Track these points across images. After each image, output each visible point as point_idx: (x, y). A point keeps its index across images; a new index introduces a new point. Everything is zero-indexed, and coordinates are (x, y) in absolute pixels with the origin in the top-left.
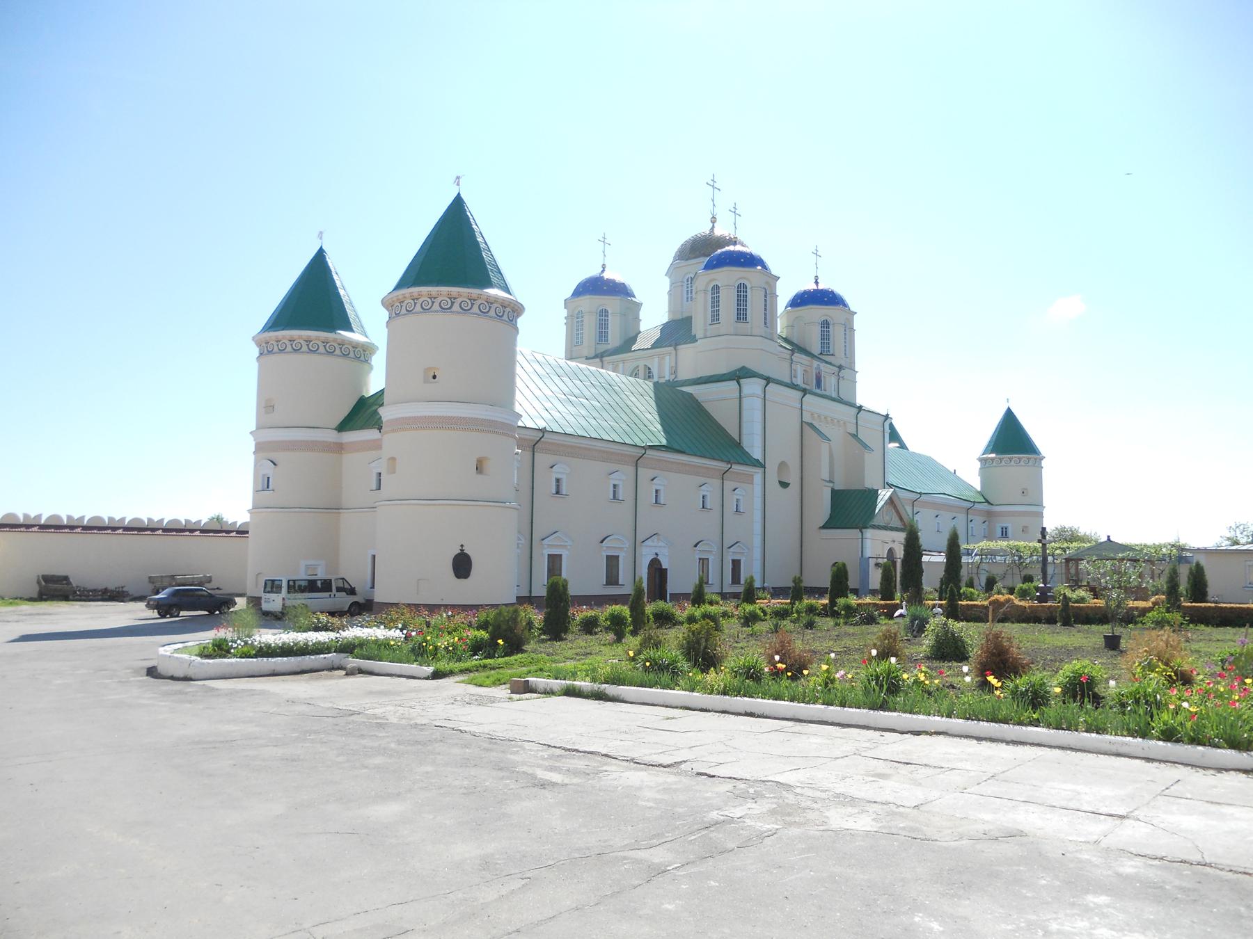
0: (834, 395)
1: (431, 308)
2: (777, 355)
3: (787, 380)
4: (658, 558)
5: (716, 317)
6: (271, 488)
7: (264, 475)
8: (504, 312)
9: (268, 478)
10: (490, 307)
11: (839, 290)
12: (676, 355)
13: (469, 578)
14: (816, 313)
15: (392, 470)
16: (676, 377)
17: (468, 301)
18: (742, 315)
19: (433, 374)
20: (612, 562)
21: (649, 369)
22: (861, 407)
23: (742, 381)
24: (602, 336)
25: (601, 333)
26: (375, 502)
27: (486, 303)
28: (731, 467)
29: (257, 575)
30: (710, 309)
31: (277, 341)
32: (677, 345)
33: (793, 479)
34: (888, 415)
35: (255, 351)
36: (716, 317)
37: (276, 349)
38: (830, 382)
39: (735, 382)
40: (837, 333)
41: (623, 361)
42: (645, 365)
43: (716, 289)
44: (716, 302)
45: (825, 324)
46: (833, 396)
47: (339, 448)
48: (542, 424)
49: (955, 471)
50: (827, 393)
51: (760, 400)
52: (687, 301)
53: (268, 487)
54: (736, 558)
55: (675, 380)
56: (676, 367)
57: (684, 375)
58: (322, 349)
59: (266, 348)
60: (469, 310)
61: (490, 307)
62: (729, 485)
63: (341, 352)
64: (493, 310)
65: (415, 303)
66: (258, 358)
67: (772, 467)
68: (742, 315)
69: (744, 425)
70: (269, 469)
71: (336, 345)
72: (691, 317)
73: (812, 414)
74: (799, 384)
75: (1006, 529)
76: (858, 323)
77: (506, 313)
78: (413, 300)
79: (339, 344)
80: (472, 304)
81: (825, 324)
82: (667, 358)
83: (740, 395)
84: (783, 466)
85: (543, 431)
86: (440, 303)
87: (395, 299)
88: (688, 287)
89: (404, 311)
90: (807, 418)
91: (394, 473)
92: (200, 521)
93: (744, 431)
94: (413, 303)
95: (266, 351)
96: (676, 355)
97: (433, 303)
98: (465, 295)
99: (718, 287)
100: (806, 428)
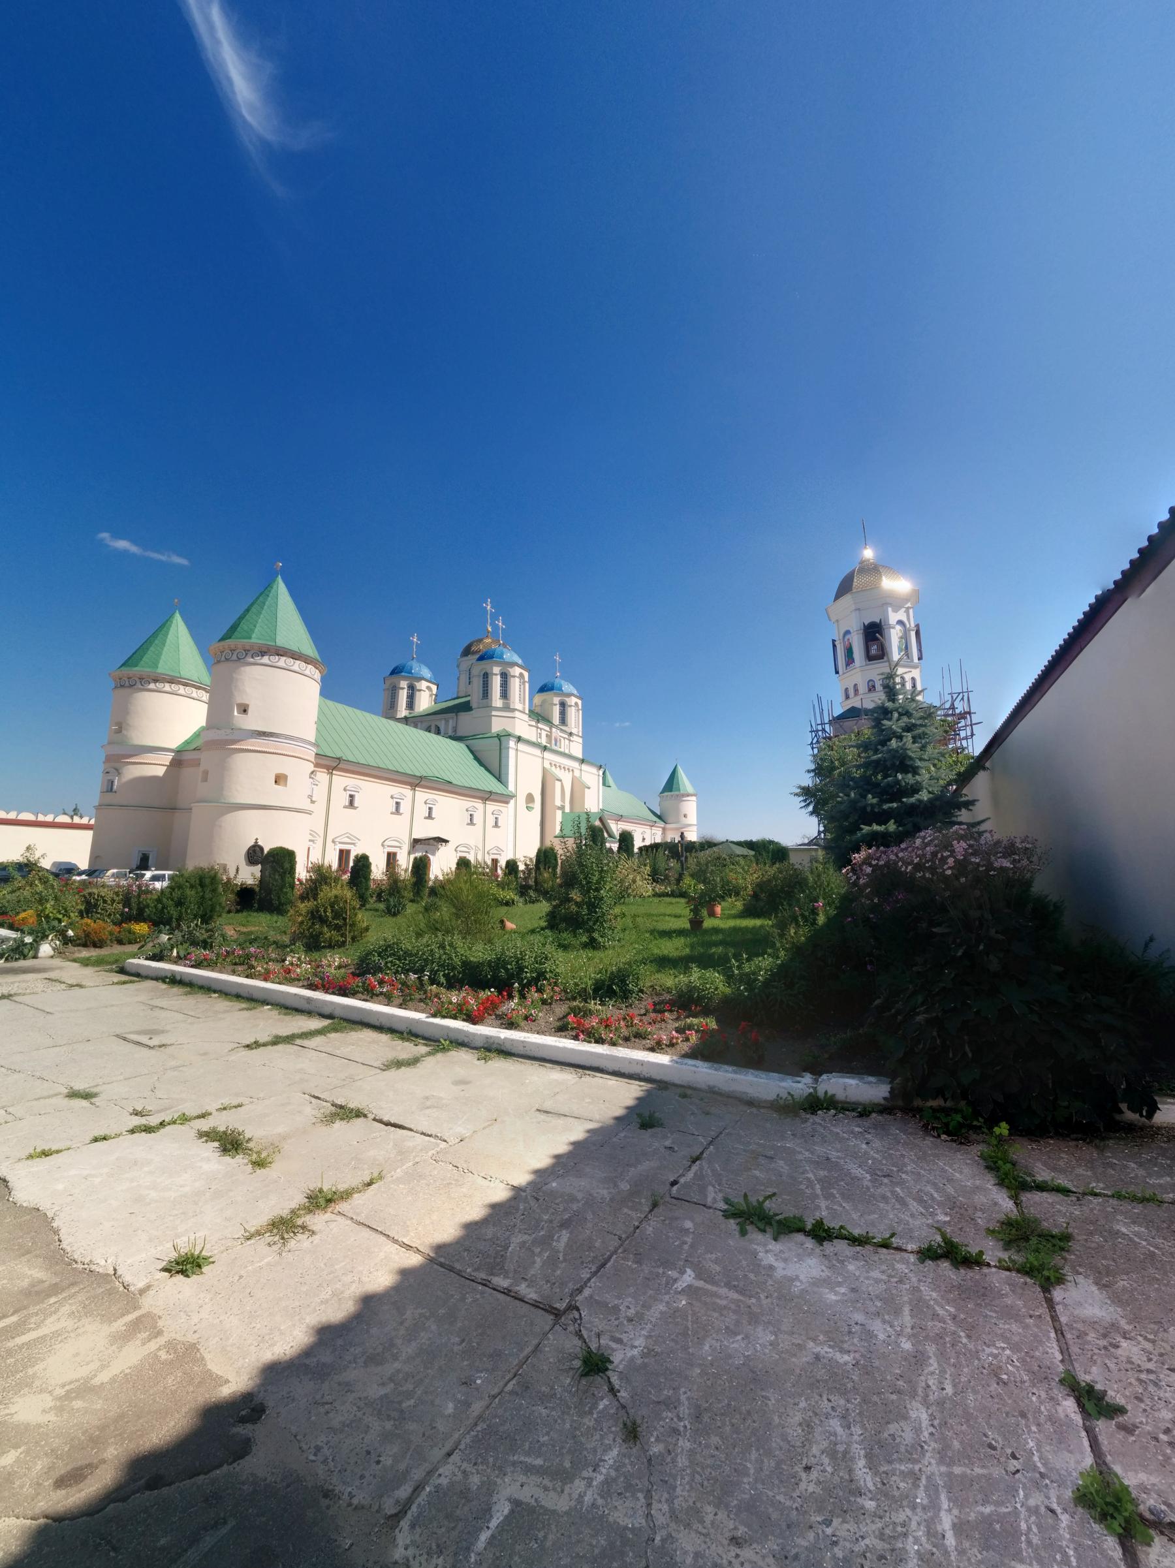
0: (567, 752)
3: (534, 739)
15: (205, 779)
18: (505, 694)
23: (502, 738)
24: (411, 705)
36: (486, 693)
41: (421, 722)
48: (338, 756)
50: (562, 750)
68: (505, 694)
69: (503, 767)
82: (451, 721)
85: (339, 759)
89: (223, 659)
90: (547, 765)
93: (503, 772)
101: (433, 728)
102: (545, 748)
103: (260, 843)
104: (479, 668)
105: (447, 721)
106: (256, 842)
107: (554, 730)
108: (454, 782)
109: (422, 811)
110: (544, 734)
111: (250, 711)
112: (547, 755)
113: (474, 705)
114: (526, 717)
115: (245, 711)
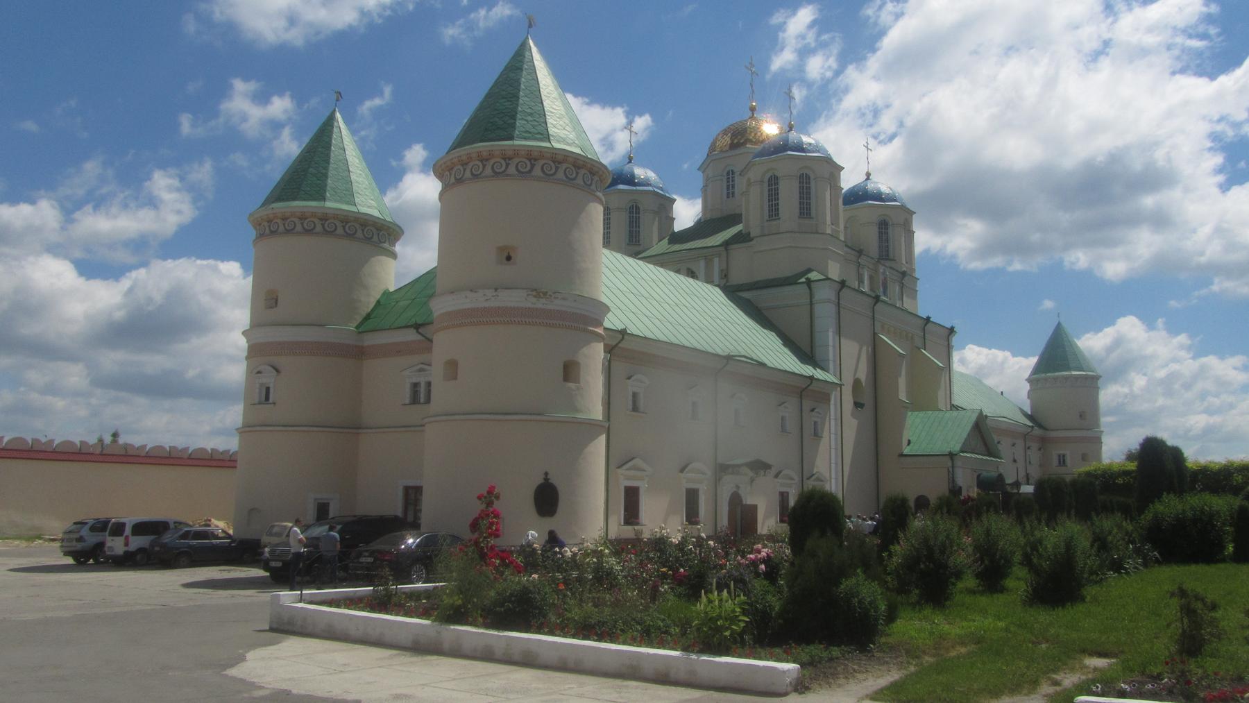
1: (505, 171)
4: (740, 492)
6: (271, 400)
7: (262, 385)
8: (592, 180)
9: (268, 389)
10: (577, 173)
13: (557, 514)
16: (727, 282)
17: (552, 164)
18: (805, 210)
19: (506, 254)
20: (692, 498)
23: (813, 285)
26: (423, 419)
29: (252, 509)
31: (283, 219)
35: (253, 233)
37: (281, 228)
39: (805, 286)
43: (774, 181)
45: (883, 226)
46: (898, 305)
47: (358, 353)
49: (1002, 393)
51: (834, 306)
52: (728, 197)
53: (267, 398)
54: (784, 489)
55: (728, 284)
58: (340, 231)
59: (267, 229)
60: (552, 175)
61: (577, 173)
62: (807, 405)
63: (364, 235)
64: (580, 176)
65: (484, 166)
66: (254, 241)
70: (269, 378)
71: (358, 226)
75: (1064, 456)
77: (594, 182)
78: (481, 161)
79: (362, 225)
80: (557, 168)
82: (716, 260)
83: (811, 302)
84: (857, 383)
86: (517, 164)
87: (455, 160)
88: (728, 182)
89: (468, 174)
91: (455, 378)
92: (188, 448)
94: (481, 166)
95: (267, 231)
97: (507, 165)
99: (776, 178)
103: (554, 480)
106: (546, 480)
108: (770, 364)
113: (754, 232)
115: (509, 258)
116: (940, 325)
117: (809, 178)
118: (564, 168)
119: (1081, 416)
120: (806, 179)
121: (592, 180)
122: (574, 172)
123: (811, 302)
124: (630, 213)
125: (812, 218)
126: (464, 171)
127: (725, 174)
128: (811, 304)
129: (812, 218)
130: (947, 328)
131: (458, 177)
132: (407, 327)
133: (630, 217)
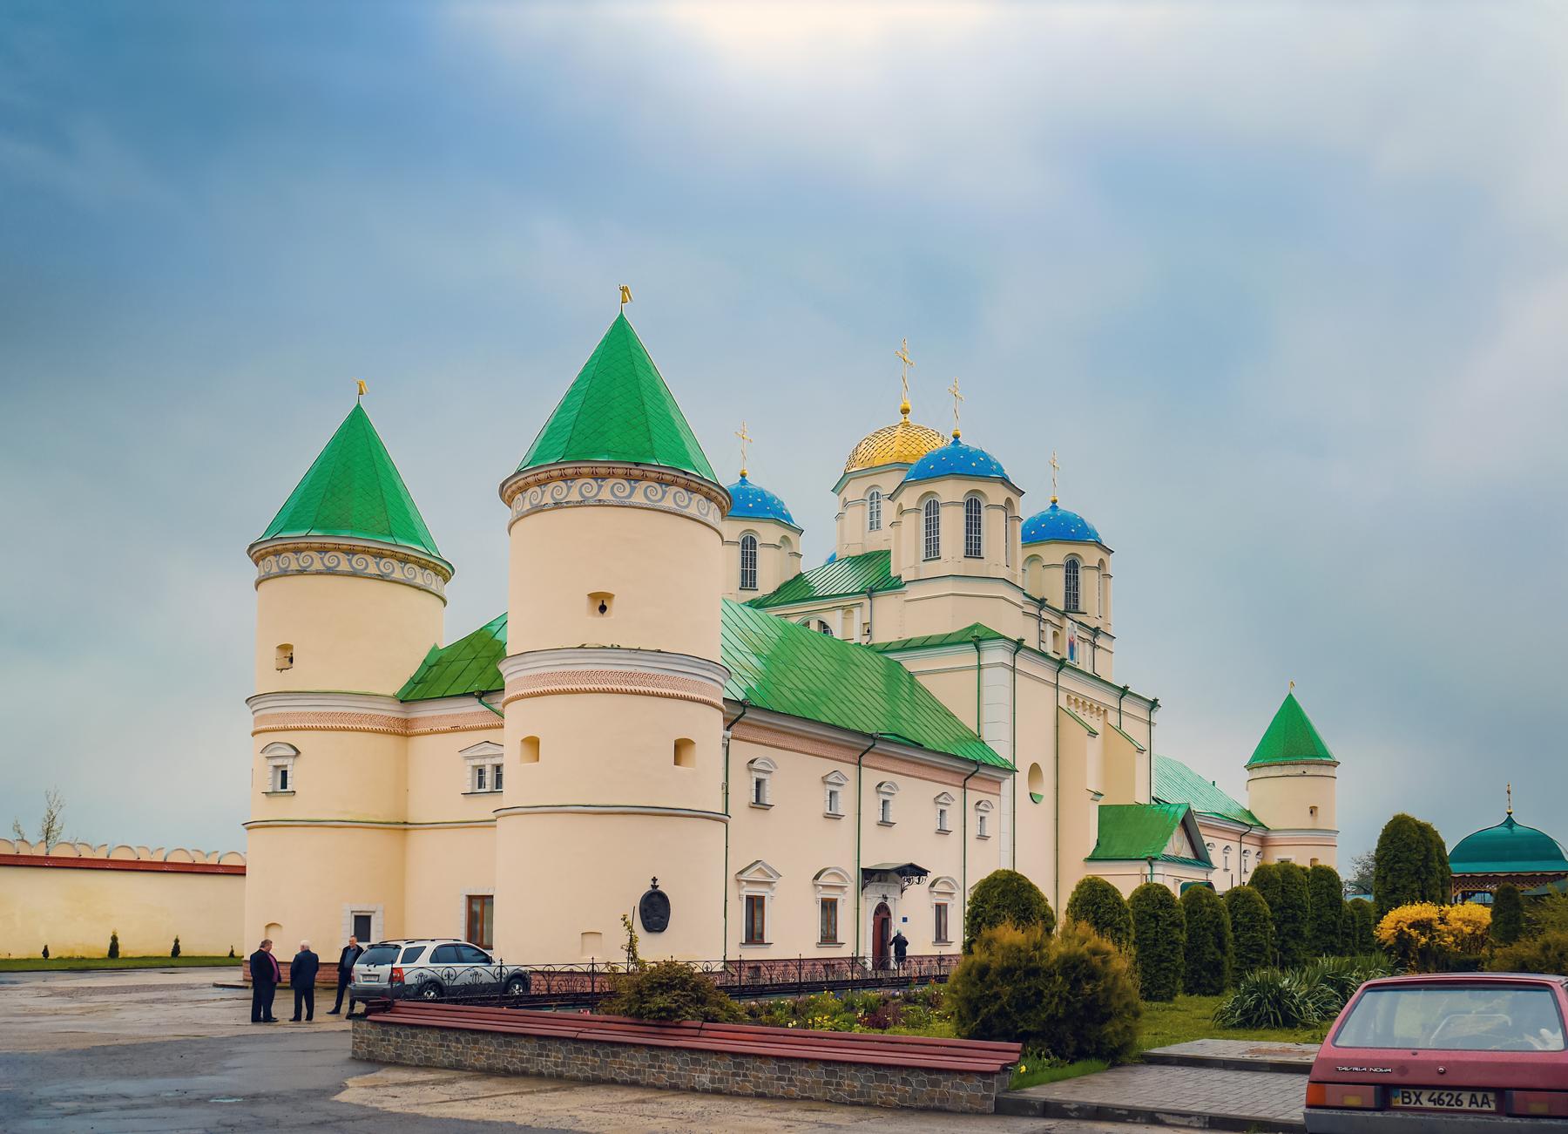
0: (1089, 671)
1: (596, 495)
2: (1022, 608)
5: (932, 550)
6: (289, 788)
8: (709, 507)
10: (690, 499)
11: (1094, 521)
12: (871, 606)
14: (1056, 554)
18: (973, 550)
21: (825, 626)
22: (1124, 691)
23: (983, 645)
25: (744, 574)
27: (684, 491)
28: (975, 772)
30: (923, 538)
32: (871, 593)
33: (1046, 789)
34: (1156, 700)
36: (932, 550)
38: (1083, 651)
39: (972, 646)
40: (1087, 580)
42: (821, 622)
43: (932, 510)
44: (932, 527)
45: (1072, 567)
51: (1008, 671)
52: (871, 529)
53: (284, 785)
56: (870, 623)
57: (882, 637)
61: (690, 499)
64: (694, 503)
67: (1023, 768)
68: (973, 550)
72: (889, 552)
73: (1068, 696)
74: (1048, 651)
76: (1112, 563)
80: (664, 493)
81: (1072, 567)
82: (856, 611)
83: (979, 665)
88: (871, 508)
90: (1063, 703)
93: (985, 718)
96: (871, 606)
98: (653, 475)
100: (1063, 716)
101: (814, 626)
102: (1061, 664)
104: (910, 498)
105: (847, 610)
107: (1068, 623)
108: (927, 746)
109: (872, 812)
110: (1049, 630)
111: (613, 607)
112: (1066, 681)
114: (1018, 598)
115: (603, 609)
116: (1140, 697)
117: (980, 507)
118: (673, 492)
119: (1311, 812)
120: (975, 507)
121: (709, 507)
122: (687, 498)
123: (979, 665)
124: (743, 548)
125: (983, 558)
126: (543, 495)
127: (868, 498)
128: (980, 667)
129: (983, 558)
130: (1149, 701)
131: (534, 502)
132: (465, 695)
133: (743, 552)
